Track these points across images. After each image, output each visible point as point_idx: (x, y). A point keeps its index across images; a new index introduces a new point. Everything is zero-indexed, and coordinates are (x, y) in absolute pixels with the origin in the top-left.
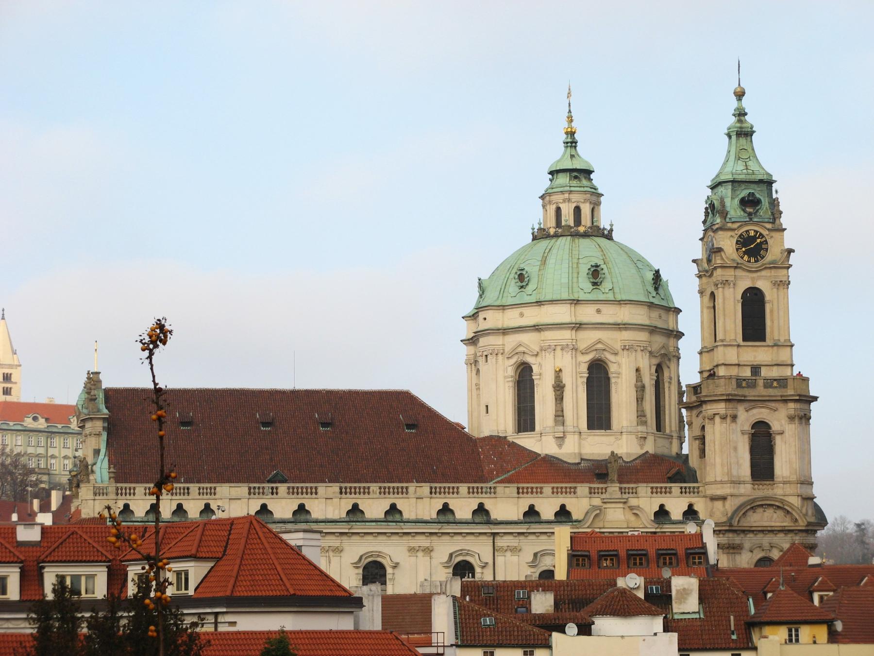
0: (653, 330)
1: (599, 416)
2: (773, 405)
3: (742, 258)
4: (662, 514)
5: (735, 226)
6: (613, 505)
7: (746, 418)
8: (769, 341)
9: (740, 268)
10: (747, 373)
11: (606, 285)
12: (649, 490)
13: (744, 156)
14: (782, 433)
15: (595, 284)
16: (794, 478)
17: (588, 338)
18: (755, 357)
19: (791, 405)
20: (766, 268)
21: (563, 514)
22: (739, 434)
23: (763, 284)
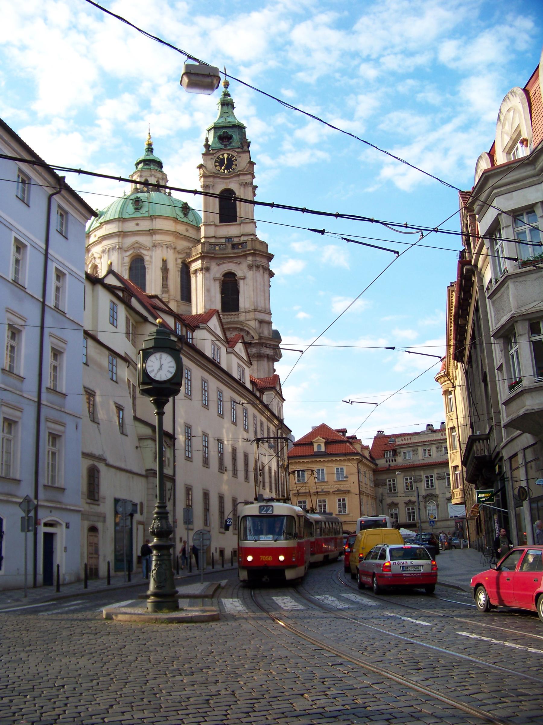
0: (177, 235)
2: (238, 260)
3: (219, 171)
5: (214, 152)
7: (218, 271)
8: (238, 222)
9: (218, 177)
13: (226, 115)
14: (244, 278)
15: (136, 209)
16: (252, 308)
17: (129, 241)
19: (250, 258)
20: (235, 176)
22: (212, 281)
23: (233, 186)
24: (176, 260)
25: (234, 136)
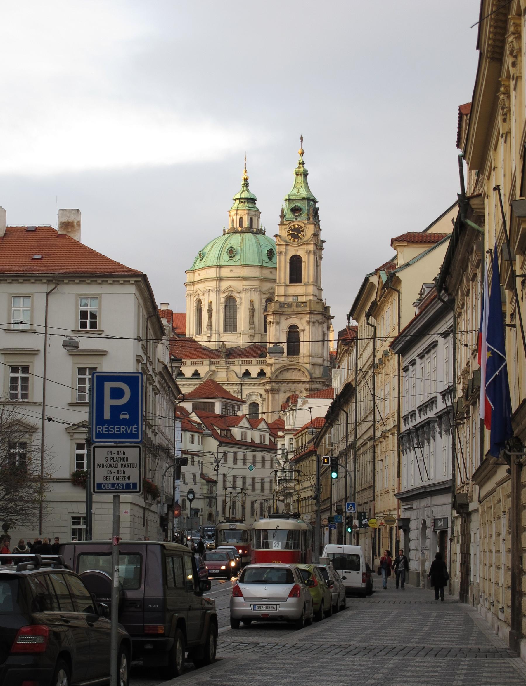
0: (263, 280)
1: (230, 325)
2: (300, 316)
4: (247, 374)
5: (288, 222)
6: (221, 370)
7: (285, 324)
8: (303, 284)
10: (290, 300)
11: (237, 257)
12: (240, 362)
15: (231, 257)
17: (225, 285)
18: (295, 291)
21: (196, 374)
22: (281, 332)
24: (261, 300)
25: (303, 208)
